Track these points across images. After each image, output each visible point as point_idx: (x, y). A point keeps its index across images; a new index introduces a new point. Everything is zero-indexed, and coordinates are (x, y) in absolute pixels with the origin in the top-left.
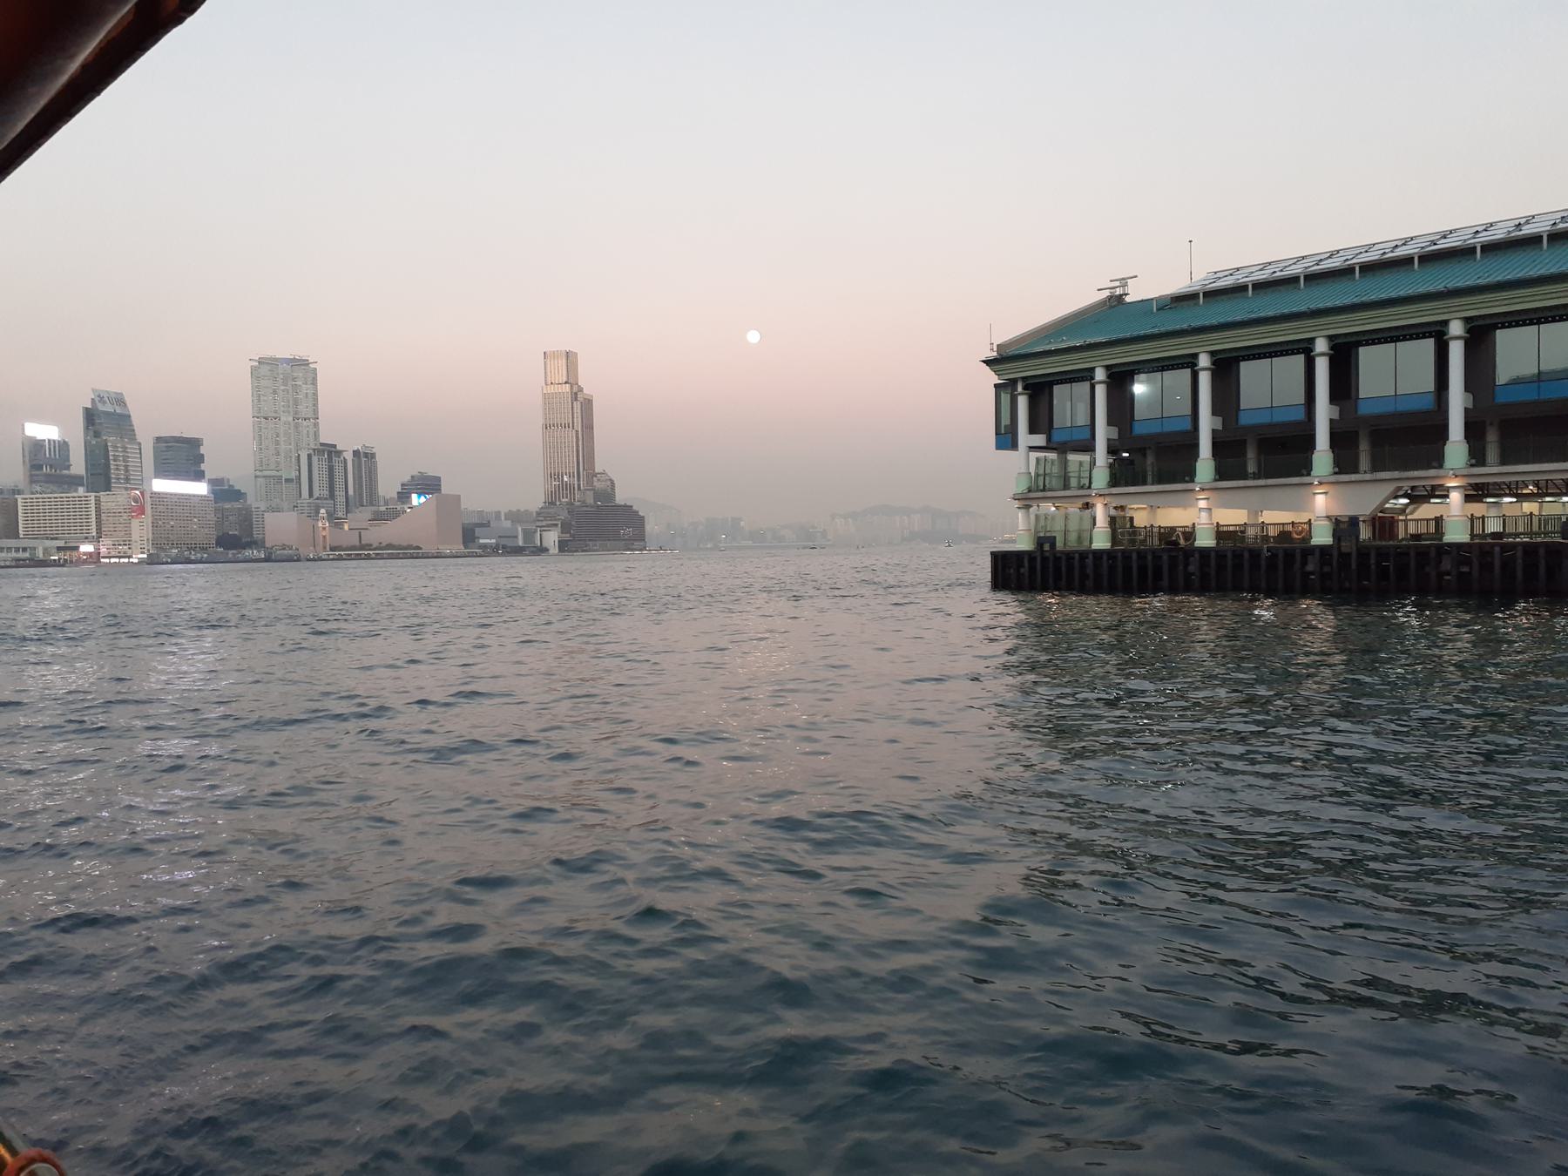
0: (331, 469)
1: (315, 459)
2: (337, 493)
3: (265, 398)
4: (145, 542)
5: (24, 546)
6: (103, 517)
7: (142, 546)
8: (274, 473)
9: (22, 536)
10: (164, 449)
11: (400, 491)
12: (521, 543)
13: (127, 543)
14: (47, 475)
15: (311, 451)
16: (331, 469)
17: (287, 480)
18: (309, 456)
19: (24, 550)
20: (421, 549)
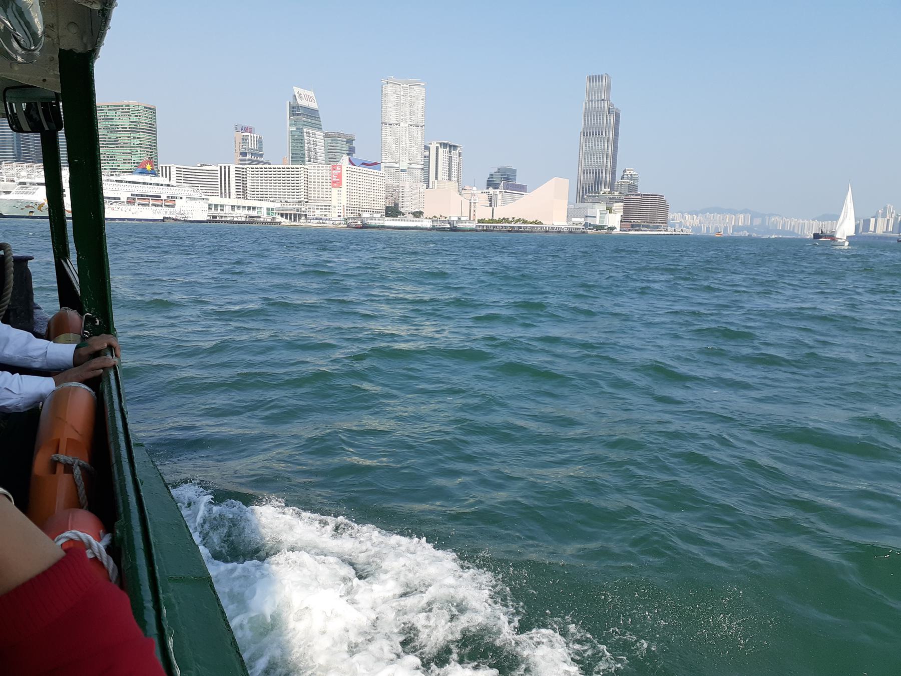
0: (450, 157)
1: (441, 150)
2: (453, 178)
3: (391, 109)
4: (342, 211)
5: (254, 206)
6: (311, 185)
7: (340, 211)
8: (395, 165)
9: (249, 198)
10: (330, 142)
11: (453, 184)
12: (598, 223)
13: (328, 207)
14: (249, 160)
15: (439, 145)
16: (450, 157)
17: (402, 171)
18: (437, 148)
19: (254, 208)
20: (542, 224)
